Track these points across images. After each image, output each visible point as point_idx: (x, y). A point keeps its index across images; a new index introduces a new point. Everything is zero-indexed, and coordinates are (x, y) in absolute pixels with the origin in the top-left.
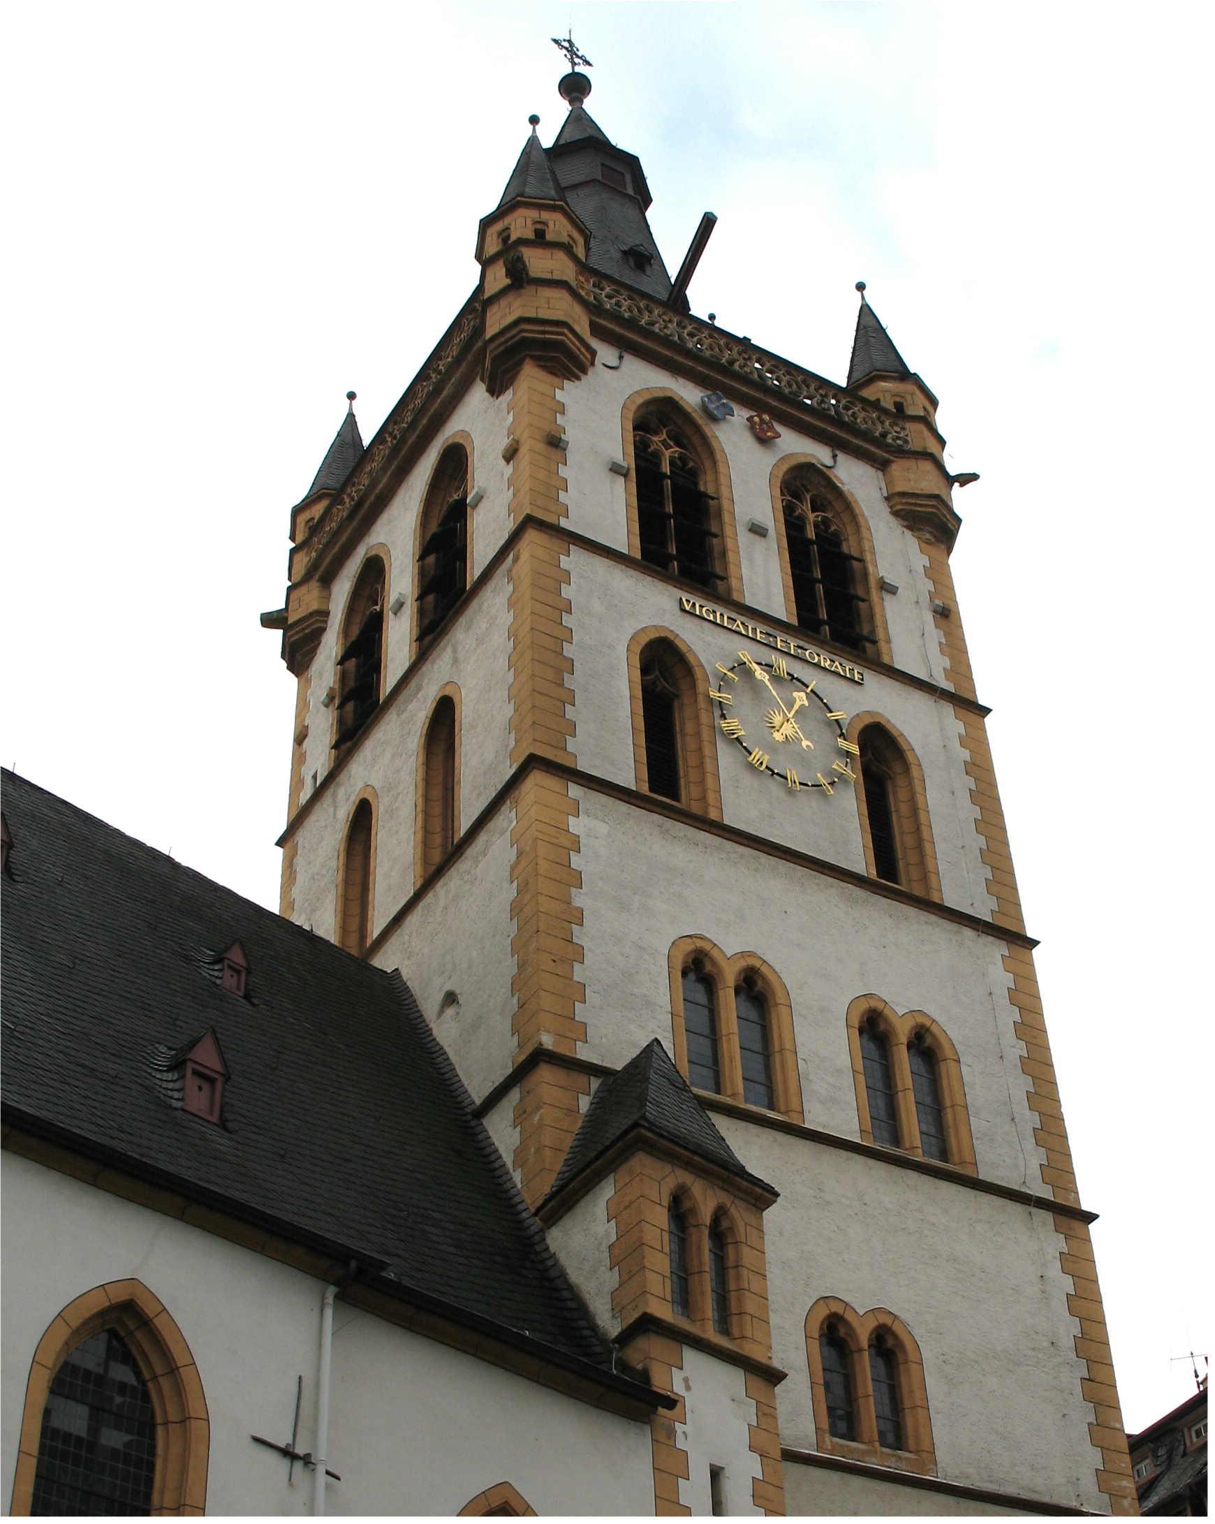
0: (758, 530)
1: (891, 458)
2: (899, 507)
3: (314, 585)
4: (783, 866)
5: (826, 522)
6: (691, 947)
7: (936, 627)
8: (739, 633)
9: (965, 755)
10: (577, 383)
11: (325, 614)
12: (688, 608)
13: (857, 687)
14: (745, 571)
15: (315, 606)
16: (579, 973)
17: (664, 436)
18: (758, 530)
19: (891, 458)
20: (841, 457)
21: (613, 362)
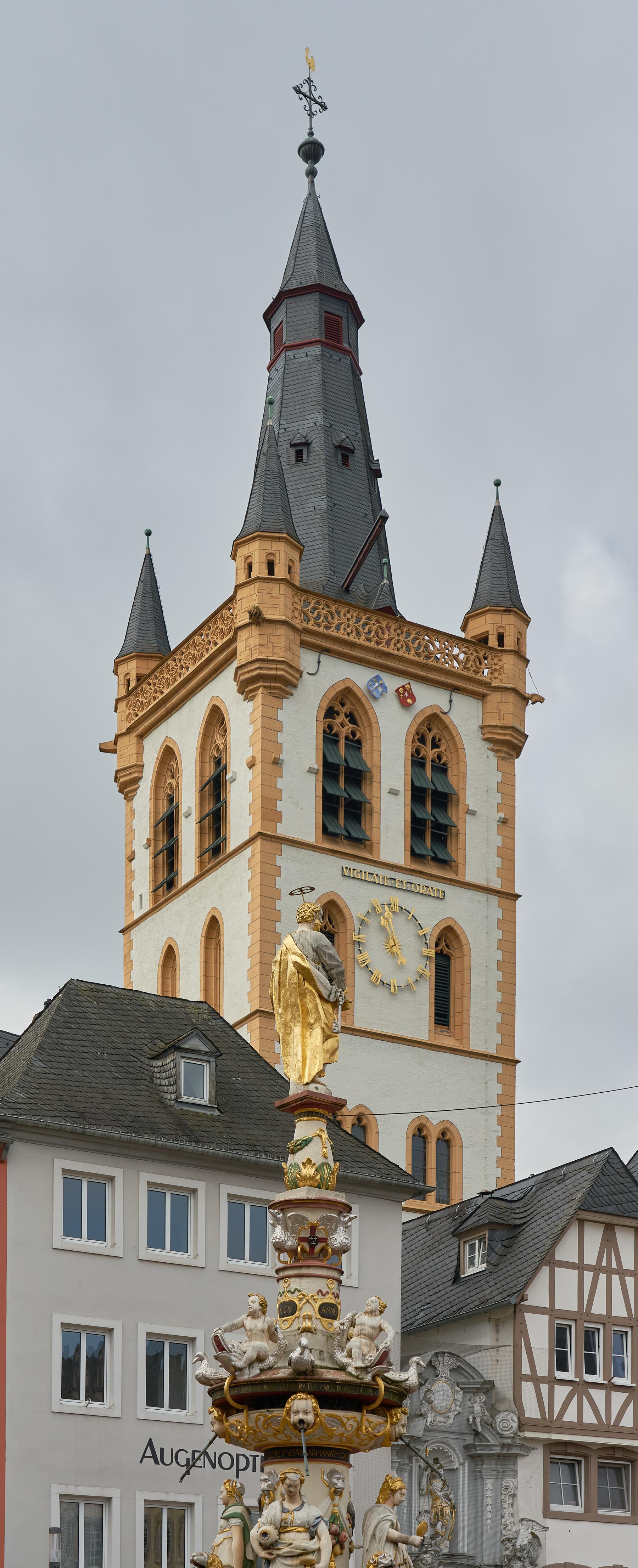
0: (393, 792)
8: (375, 883)
17: (342, 716)
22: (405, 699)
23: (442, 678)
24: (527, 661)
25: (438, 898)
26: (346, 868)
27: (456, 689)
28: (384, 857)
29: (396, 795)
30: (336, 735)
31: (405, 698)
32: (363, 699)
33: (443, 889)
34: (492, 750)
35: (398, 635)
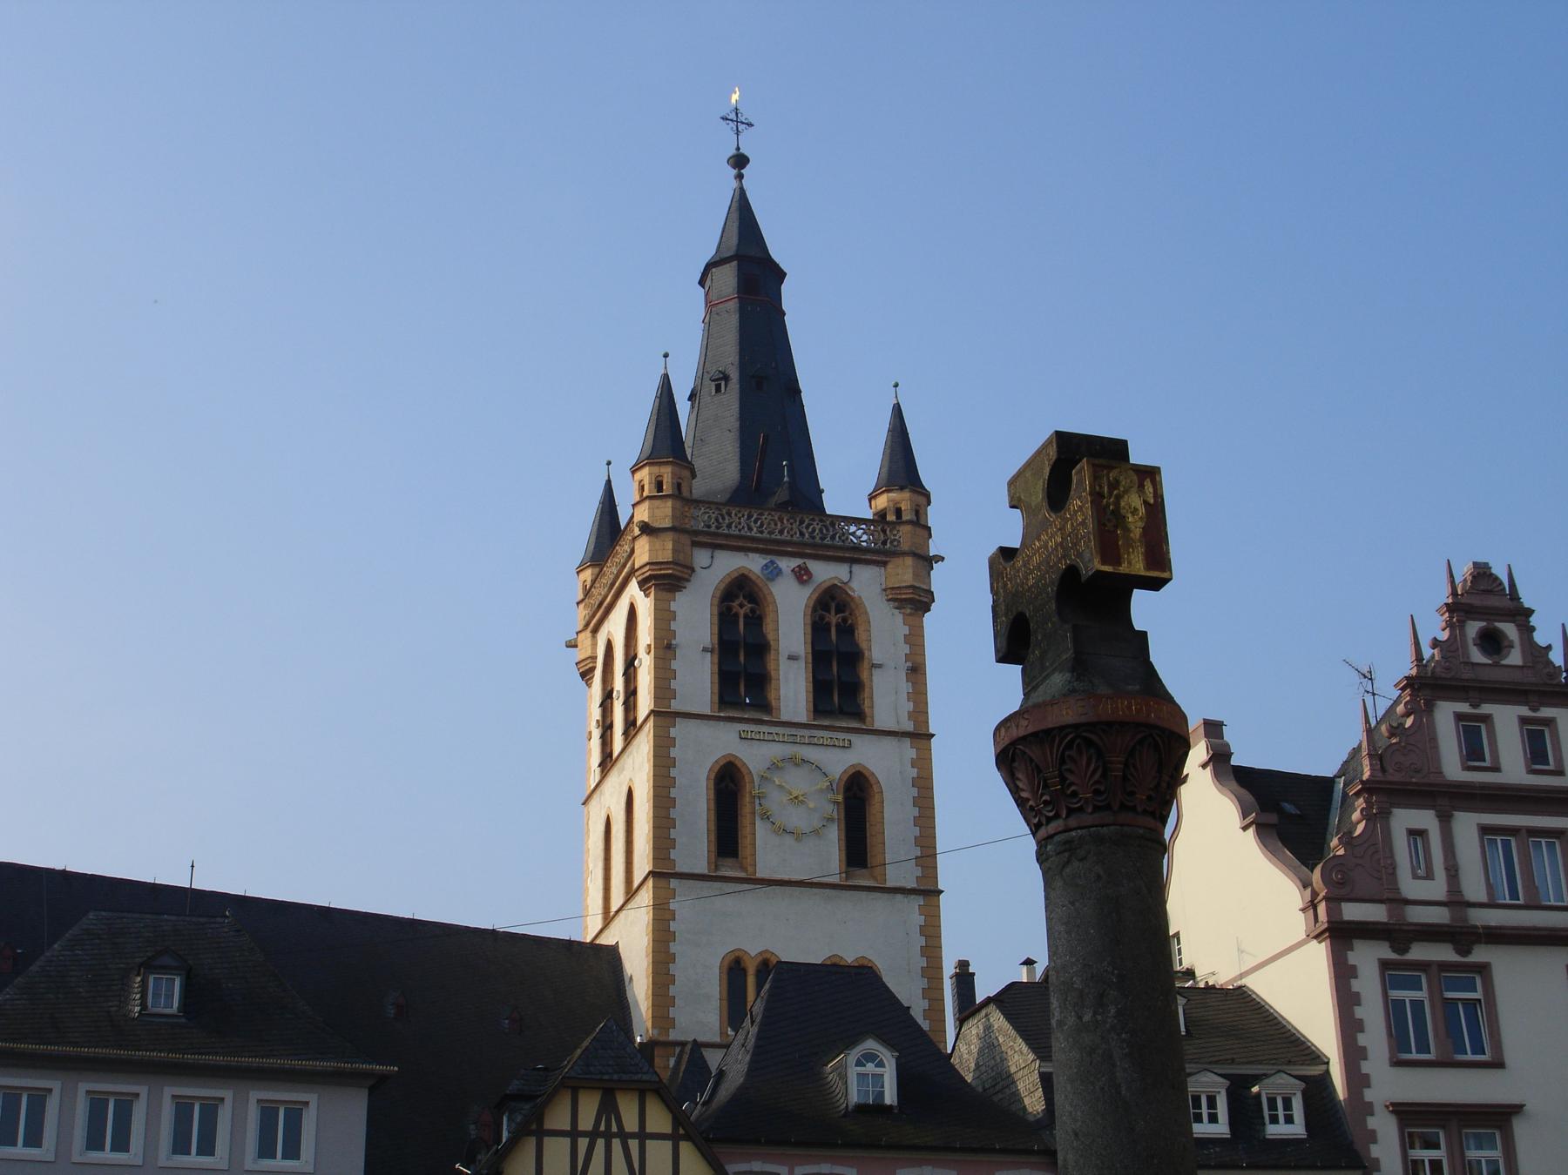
1: (888, 559)
2: (890, 597)
3: (588, 633)
4: (788, 889)
5: (845, 620)
6: (733, 957)
7: (907, 681)
9: (914, 772)
10: (684, 590)
11: (596, 657)
12: (743, 736)
13: (847, 750)
14: (782, 692)
15: (589, 653)
16: (672, 990)
17: (741, 598)
18: (792, 658)
19: (888, 559)
20: (856, 568)
21: (706, 562)
22: (802, 575)
23: (840, 554)
24: (929, 529)
25: (843, 747)
26: (744, 731)
27: (853, 561)
28: (784, 717)
29: (797, 659)
30: (736, 615)
31: (801, 576)
32: (758, 581)
33: (849, 738)
34: (896, 608)
35: (791, 524)
